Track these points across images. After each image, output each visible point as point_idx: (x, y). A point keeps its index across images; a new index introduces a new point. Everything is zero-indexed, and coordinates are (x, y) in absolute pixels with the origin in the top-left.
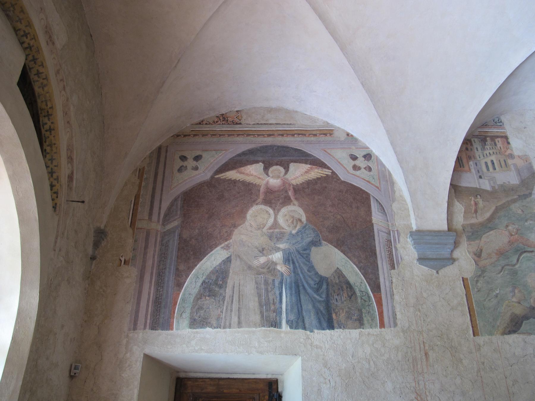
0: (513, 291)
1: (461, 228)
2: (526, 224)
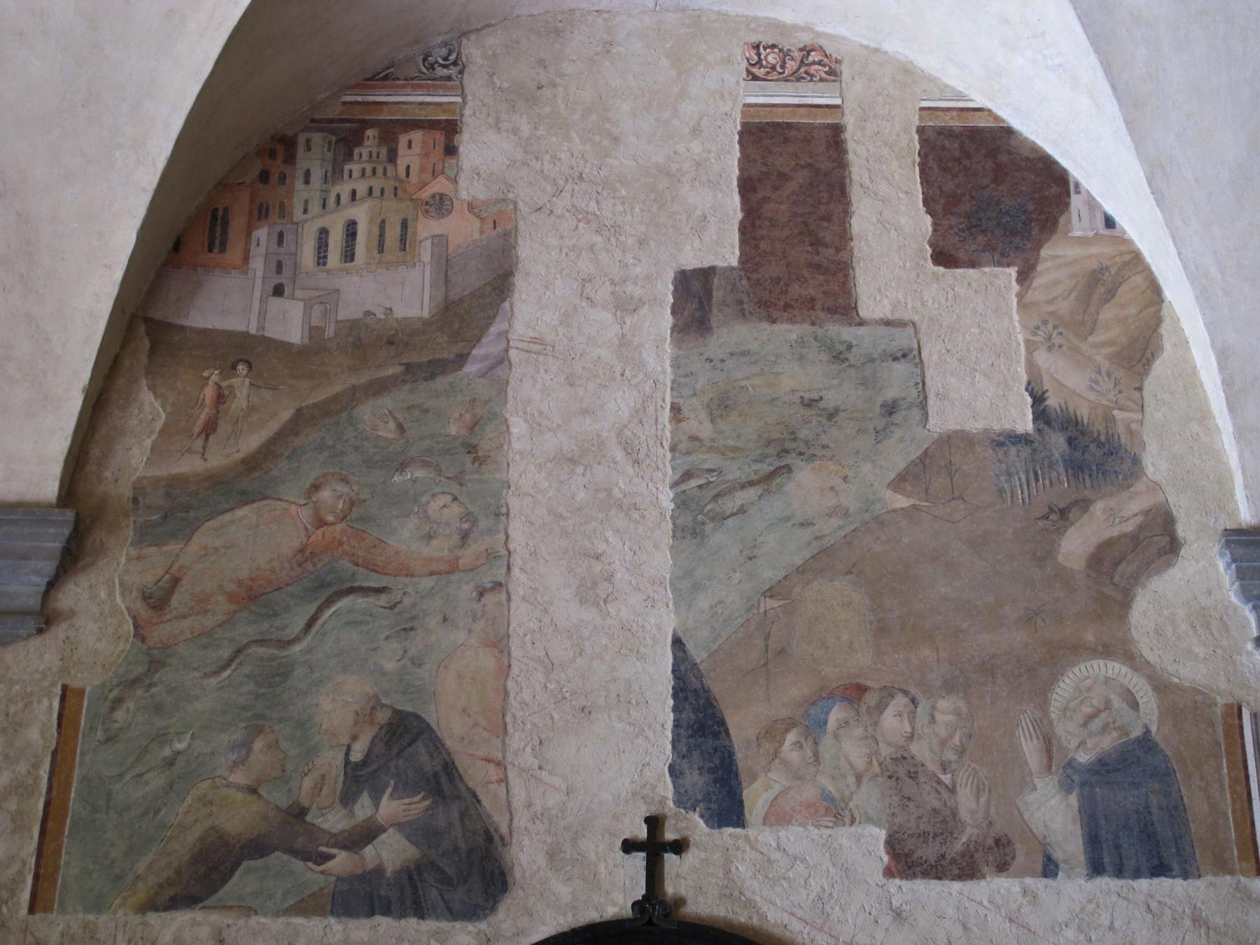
0: (247, 745)
1: (128, 493)
2: (397, 478)
